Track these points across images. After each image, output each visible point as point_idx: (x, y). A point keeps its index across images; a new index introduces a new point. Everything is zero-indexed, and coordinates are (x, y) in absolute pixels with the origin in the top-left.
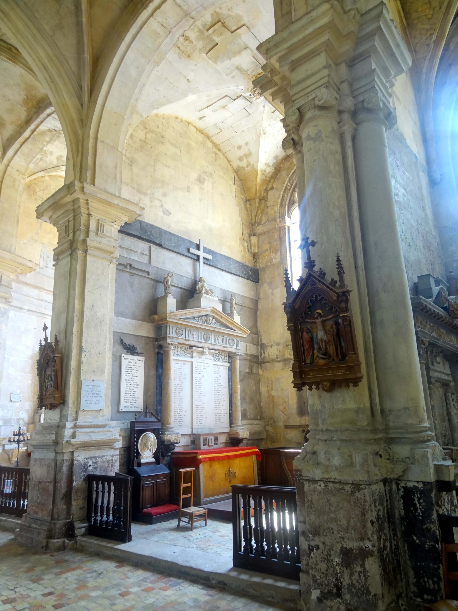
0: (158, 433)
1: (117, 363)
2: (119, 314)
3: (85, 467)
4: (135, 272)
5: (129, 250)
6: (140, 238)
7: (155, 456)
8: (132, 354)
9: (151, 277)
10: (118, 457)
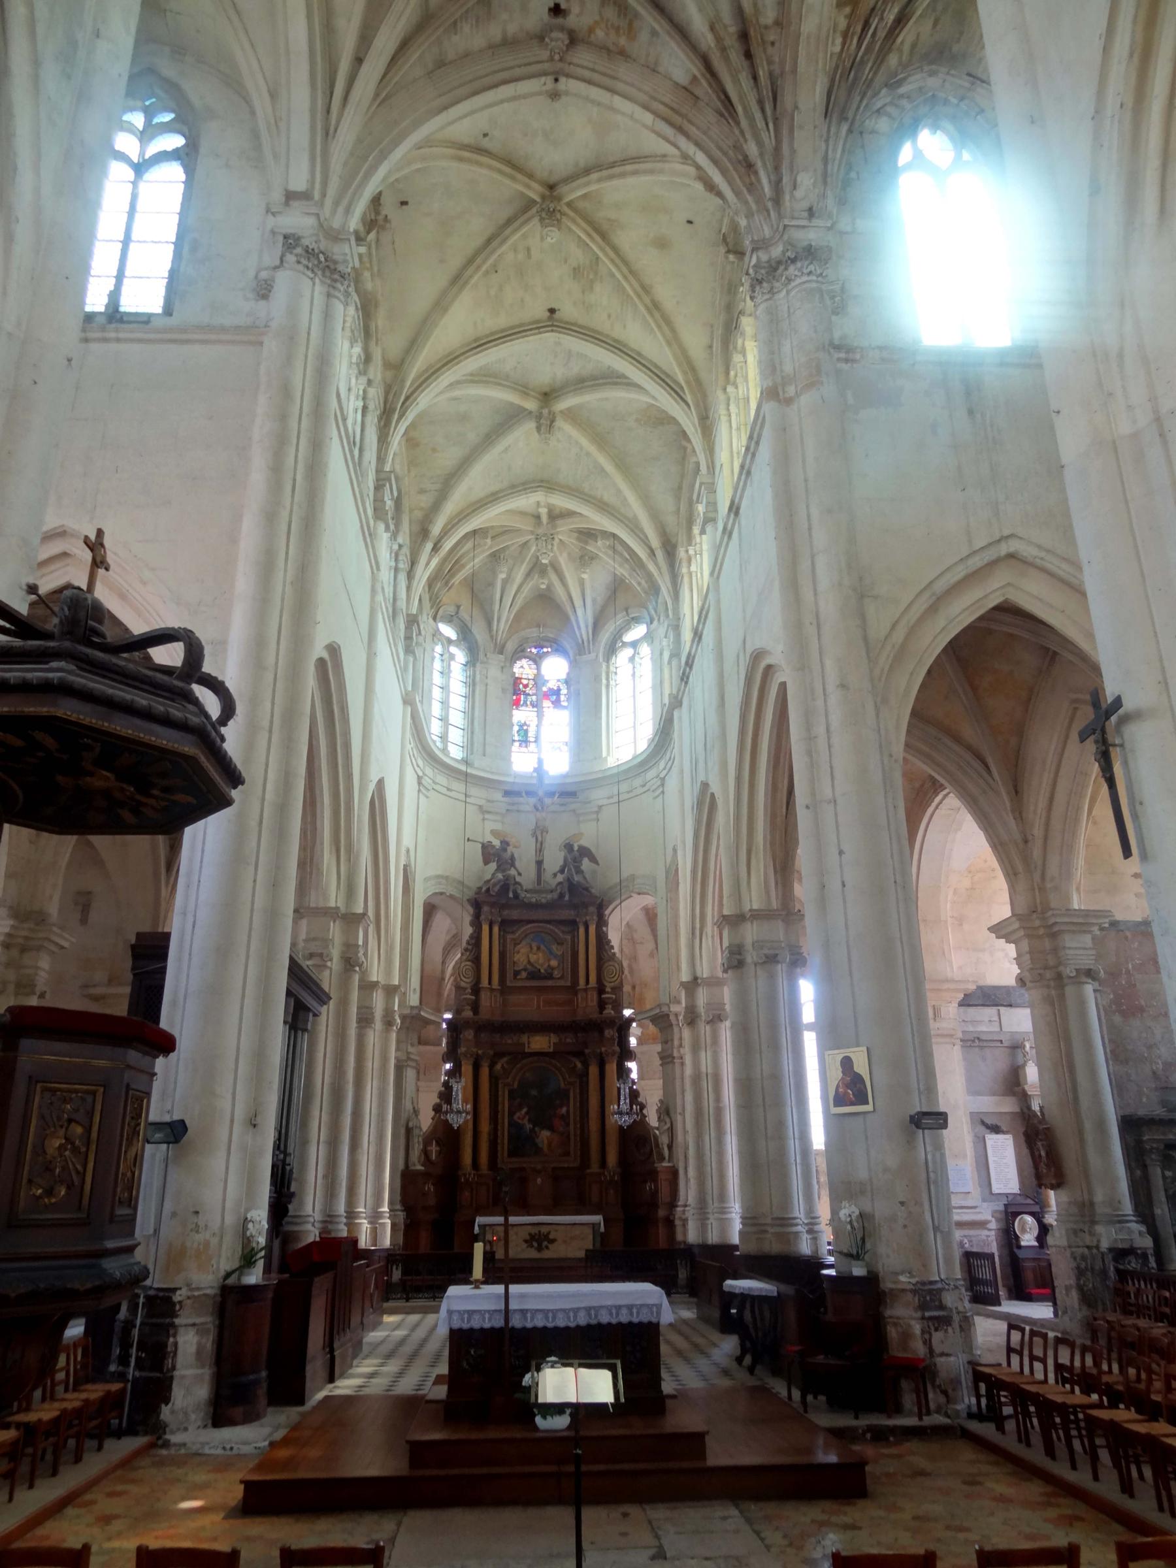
0: (1038, 1217)
2: (973, 1091)
3: (961, 1244)
5: (973, 1022)
6: (983, 1005)
9: (1006, 1044)
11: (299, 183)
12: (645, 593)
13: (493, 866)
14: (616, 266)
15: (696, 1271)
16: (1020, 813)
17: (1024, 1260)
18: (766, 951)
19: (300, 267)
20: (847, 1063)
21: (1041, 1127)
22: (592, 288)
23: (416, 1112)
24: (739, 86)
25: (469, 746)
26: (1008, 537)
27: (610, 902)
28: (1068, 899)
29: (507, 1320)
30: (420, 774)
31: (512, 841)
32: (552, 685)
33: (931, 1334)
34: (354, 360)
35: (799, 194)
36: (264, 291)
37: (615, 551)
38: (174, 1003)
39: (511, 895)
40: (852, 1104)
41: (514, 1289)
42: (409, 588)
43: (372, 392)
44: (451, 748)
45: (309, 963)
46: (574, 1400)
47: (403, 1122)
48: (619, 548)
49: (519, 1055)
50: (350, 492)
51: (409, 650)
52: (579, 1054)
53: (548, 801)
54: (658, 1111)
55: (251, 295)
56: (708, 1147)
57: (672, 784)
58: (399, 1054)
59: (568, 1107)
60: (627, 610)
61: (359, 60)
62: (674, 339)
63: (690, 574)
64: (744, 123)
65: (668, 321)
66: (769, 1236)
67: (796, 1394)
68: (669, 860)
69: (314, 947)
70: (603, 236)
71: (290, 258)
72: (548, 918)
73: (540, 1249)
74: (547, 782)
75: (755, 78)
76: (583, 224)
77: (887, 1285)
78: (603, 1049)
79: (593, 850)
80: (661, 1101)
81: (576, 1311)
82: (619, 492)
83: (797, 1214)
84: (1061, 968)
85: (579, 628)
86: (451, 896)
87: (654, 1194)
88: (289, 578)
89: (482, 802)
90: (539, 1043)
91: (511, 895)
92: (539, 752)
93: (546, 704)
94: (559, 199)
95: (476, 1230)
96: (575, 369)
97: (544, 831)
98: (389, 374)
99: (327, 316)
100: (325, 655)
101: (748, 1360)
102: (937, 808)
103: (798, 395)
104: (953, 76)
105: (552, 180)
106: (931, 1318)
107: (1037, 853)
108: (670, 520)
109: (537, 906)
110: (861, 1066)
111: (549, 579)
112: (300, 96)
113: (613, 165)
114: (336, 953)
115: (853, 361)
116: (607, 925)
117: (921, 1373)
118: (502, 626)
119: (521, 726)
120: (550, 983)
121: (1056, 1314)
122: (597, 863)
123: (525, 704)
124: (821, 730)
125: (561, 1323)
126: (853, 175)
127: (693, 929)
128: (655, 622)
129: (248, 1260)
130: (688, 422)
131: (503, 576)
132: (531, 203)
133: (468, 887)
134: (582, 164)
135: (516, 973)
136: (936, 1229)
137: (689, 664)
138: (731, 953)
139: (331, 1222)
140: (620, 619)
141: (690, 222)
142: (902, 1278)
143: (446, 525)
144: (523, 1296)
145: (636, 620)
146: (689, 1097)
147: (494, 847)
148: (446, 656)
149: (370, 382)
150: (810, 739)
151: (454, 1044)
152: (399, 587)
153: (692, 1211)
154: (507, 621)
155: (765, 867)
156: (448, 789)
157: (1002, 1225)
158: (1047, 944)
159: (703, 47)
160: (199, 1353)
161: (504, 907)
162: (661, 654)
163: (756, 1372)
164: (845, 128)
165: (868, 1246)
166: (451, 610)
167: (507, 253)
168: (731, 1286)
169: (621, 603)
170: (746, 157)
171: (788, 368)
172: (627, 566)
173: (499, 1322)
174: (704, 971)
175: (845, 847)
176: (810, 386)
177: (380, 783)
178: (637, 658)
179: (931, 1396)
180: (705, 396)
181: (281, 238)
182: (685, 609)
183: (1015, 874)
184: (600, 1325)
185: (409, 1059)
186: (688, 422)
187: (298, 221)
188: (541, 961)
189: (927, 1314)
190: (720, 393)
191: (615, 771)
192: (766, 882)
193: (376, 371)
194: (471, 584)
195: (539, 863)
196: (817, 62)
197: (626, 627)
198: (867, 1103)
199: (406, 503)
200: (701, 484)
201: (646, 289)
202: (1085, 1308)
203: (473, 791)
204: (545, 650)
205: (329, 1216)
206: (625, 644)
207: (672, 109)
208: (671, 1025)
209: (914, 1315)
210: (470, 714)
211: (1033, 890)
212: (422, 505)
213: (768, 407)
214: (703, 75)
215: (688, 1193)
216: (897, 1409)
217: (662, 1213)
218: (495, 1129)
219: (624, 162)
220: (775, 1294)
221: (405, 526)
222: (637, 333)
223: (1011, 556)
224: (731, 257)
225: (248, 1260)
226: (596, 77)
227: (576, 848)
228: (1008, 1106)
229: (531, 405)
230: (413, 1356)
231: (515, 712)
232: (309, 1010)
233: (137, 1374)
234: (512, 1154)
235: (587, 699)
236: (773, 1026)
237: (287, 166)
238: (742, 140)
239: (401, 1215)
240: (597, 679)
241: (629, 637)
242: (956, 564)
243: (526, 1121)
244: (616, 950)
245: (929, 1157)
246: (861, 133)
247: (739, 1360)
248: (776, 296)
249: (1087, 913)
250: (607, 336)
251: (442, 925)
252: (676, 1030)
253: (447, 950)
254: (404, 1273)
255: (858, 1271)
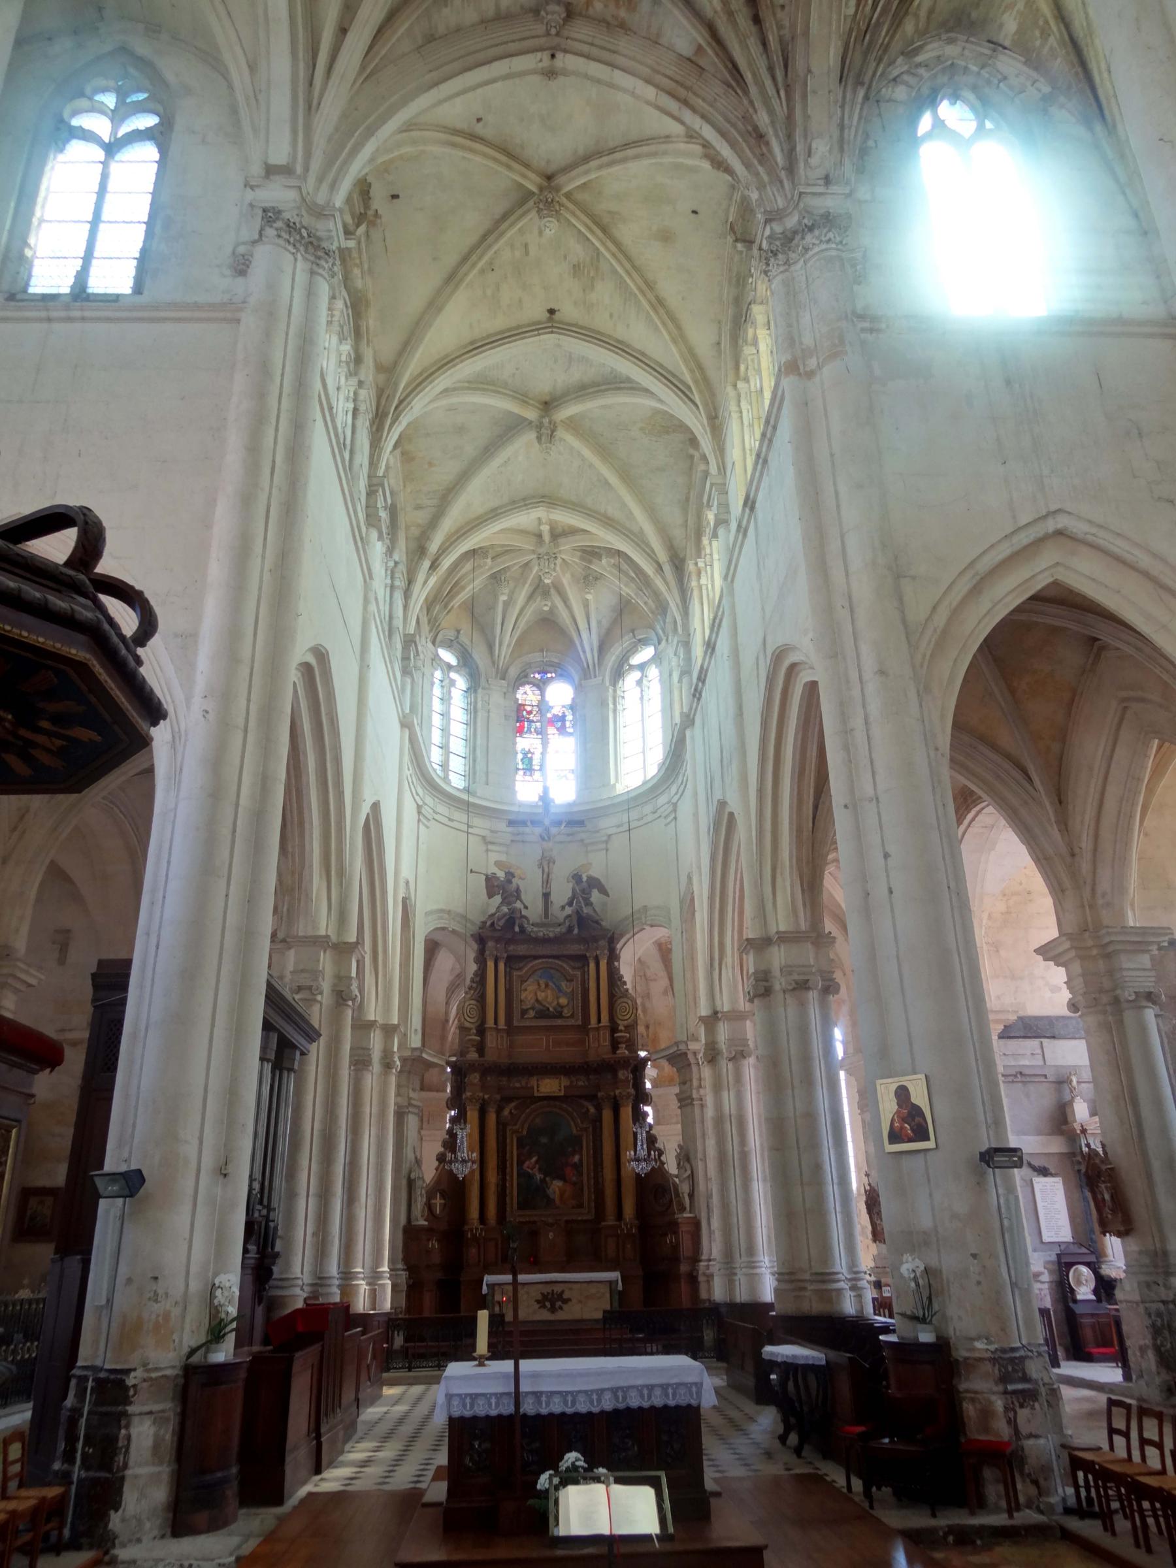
0: (1094, 1267)
1: (1029, 1189)
4: (1028, 1079)
7: (1095, 1292)
8: (1045, 1176)
9: (1051, 1079)
10: (1047, 1292)
11: (279, 156)
12: (653, 613)
13: (498, 899)
14: (618, 260)
15: (730, 1333)
16: (1066, 825)
17: (1082, 1315)
18: (796, 977)
19: (281, 242)
20: (902, 1094)
21: (1104, 1167)
22: (592, 287)
23: (418, 1162)
24: (747, 52)
25: (471, 774)
26: (1055, 512)
27: (622, 936)
28: (1122, 915)
29: (517, 1404)
30: (420, 803)
31: (517, 873)
32: (557, 711)
33: (1015, 1413)
34: (344, 358)
35: (814, 161)
36: (241, 267)
37: (620, 570)
38: (134, 1036)
39: (517, 929)
40: (910, 1140)
41: (526, 1365)
42: (406, 607)
43: (363, 393)
44: (452, 776)
45: (297, 997)
46: (607, 1532)
47: (404, 1172)
48: (625, 567)
49: (529, 1099)
50: (339, 489)
51: (406, 672)
52: (592, 1098)
53: (554, 830)
54: (678, 1157)
55: (228, 272)
56: (733, 1195)
57: (685, 808)
58: (399, 1099)
59: (581, 1155)
60: (633, 631)
61: (343, 31)
62: (679, 336)
63: (700, 587)
64: (753, 90)
65: (673, 319)
66: (807, 1294)
67: (857, 1485)
68: (683, 889)
69: (304, 980)
70: (604, 230)
71: (270, 232)
72: (554, 953)
73: (553, 1310)
74: (553, 810)
75: (764, 44)
76: (583, 217)
77: (961, 1353)
78: (617, 1092)
79: (603, 881)
80: (680, 1146)
81: (600, 1392)
82: (624, 505)
83: (837, 1269)
84: (1119, 992)
85: (584, 652)
86: (454, 932)
87: (676, 1247)
88: (266, 569)
89: (483, 833)
90: (549, 1086)
91: (517, 929)
92: (545, 780)
93: (551, 730)
94: (557, 189)
95: (485, 1287)
96: (577, 375)
97: (551, 861)
98: (382, 378)
99: (310, 293)
100: (312, 660)
101: (793, 1439)
102: (969, 826)
103: (819, 367)
104: (972, 43)
105: (549, 171)
106: (1014, 1392)
107: (1085, 867)
108: (678, 533)
109: (546, 941)
110: (919, 1096)
111: (553, 602)
112: (280, 66)
113: (612, 151)
114: (326, 985)
115: (878, 331)
116: (619, 961)
117: (1006, 1458)
118: (504, 651)
119: (525, 754)
120: (559, 1022)
121: (1127, 1377)
122: (608, 895)
123: (529, 730)
124: (858, 722)
125: (582, 1407)
126: (871, 143)
127: (712, 959)
128: (664, 643)
129: (216, 1334)
130: (696, 422)
131: (505, 598)
132: (527, 195)
133: (473, 923)
134: (581, 151)
135: (524, 1012)
136: (1014, 1285)
137: (702, 678)
138: (757, 980)
139: (321, 1285)
140: (627, 641)
141: (695, 212)
142: (979, 1345)
143: (443, 544)
144: (535, 1376)
145: (644, 642)
146: (711, 1143)
147: (498, 878)
148: (446, 682)
149: (361, 384)
150: (846, 732)
151: (458, 1090)
152: (395, 606)
153: (717, 1267)
154: (509, 646)
155: (792, 886)
156: (450, 820)
157: (1056, 1277)
158: (1101, 965)
159: (709, 13)
160: (156, 1447)
161: (509, 942)
162: (670, 675)
163: (804, 1454)
164: (861, 93)
165: (936, 1307)
166: (451, 634)
167: (503, 250)
168: (772, 1354)
169: (628, 624)
170: (756, 128)
171: (808, 341)
172: (632, 585)
173: (507, 1409)
174: (725, 1005)
175: (891, 849)
176: (834, 356)
177: (376, 807)
178: (645, 682)
179: (1019, 1486)
180: (713, 395)
181: (260, 212)
182: (696, 623)
183: (1063, 891)
184: (628, 1409)
185: (410, 1105)
186: (696, 422)
187: (279, 194)
188: (549, 999)
189: (1010, 1387)
190: (729, 389)
191: (625, 797)
192: (793, 902)
193: (368, 372)
194: (470, 608)
195: (546, 896)
196: (830, 24)
197: (633, 650)
198: (928, 1139)
199: (402, 520)
200: (712, 485)
201: (650, 285)
202: (1163, 1371)
203: (476, 821)
204: (549, 675)
205: (320, 1278)
206: (632, 667)
207: (677, 82)
208: (689, 1065)
209: (995, 1389)
210: (471, 742)
211: (1083, 906)
212: (420, 521)
213: (786, 382)
214: (709, 44)
215: (712, 1247)
216: (979, 1504)
217: (684, 1268)
218: (504, 1180)
219: (626, 146)
220: (824, 1363)
221: (402, 543)
222: (639, 331)
223: (1060, 533)
224: (739, 246)
225: (216, 1334)
226: (595, 51)
227: (585, 879)
228: (1056, 1146)
229: (531, 414)
230: (414, 1438)
231: (519, 739)
232: (295, 1047)
233: (83, 1474)
234: (521, 1206)
235: (595, 730)
236: (806, 1059)
237: (267, 141)
238: (751, 110)
239: (404, 1275)
240: (604, 704)
241: (636, 660)
242: (999, 541)
243: (536, 1170)
244: (629, 986)
245: (1002, 1201)
246: (878, 101)
247: (783, 1439)
248: (793, 268)
249: (1143, 931)
250: (609, 336)
251: (445, 963)
252: (694, 1069)
253: (451, 991)
254: (406, 1340)
255: (926, 1336)
